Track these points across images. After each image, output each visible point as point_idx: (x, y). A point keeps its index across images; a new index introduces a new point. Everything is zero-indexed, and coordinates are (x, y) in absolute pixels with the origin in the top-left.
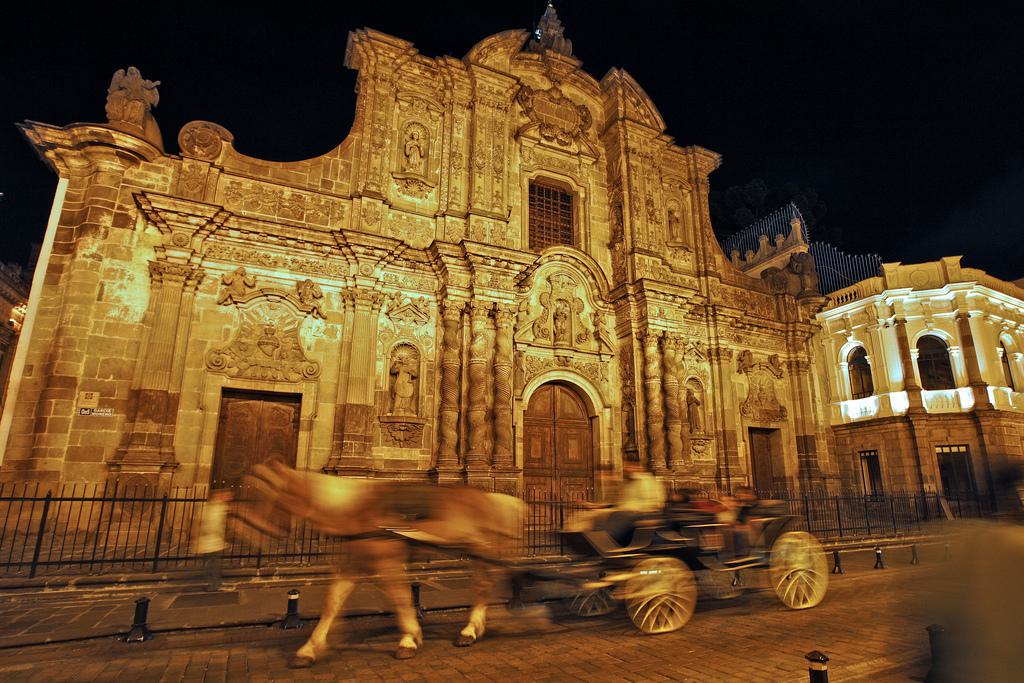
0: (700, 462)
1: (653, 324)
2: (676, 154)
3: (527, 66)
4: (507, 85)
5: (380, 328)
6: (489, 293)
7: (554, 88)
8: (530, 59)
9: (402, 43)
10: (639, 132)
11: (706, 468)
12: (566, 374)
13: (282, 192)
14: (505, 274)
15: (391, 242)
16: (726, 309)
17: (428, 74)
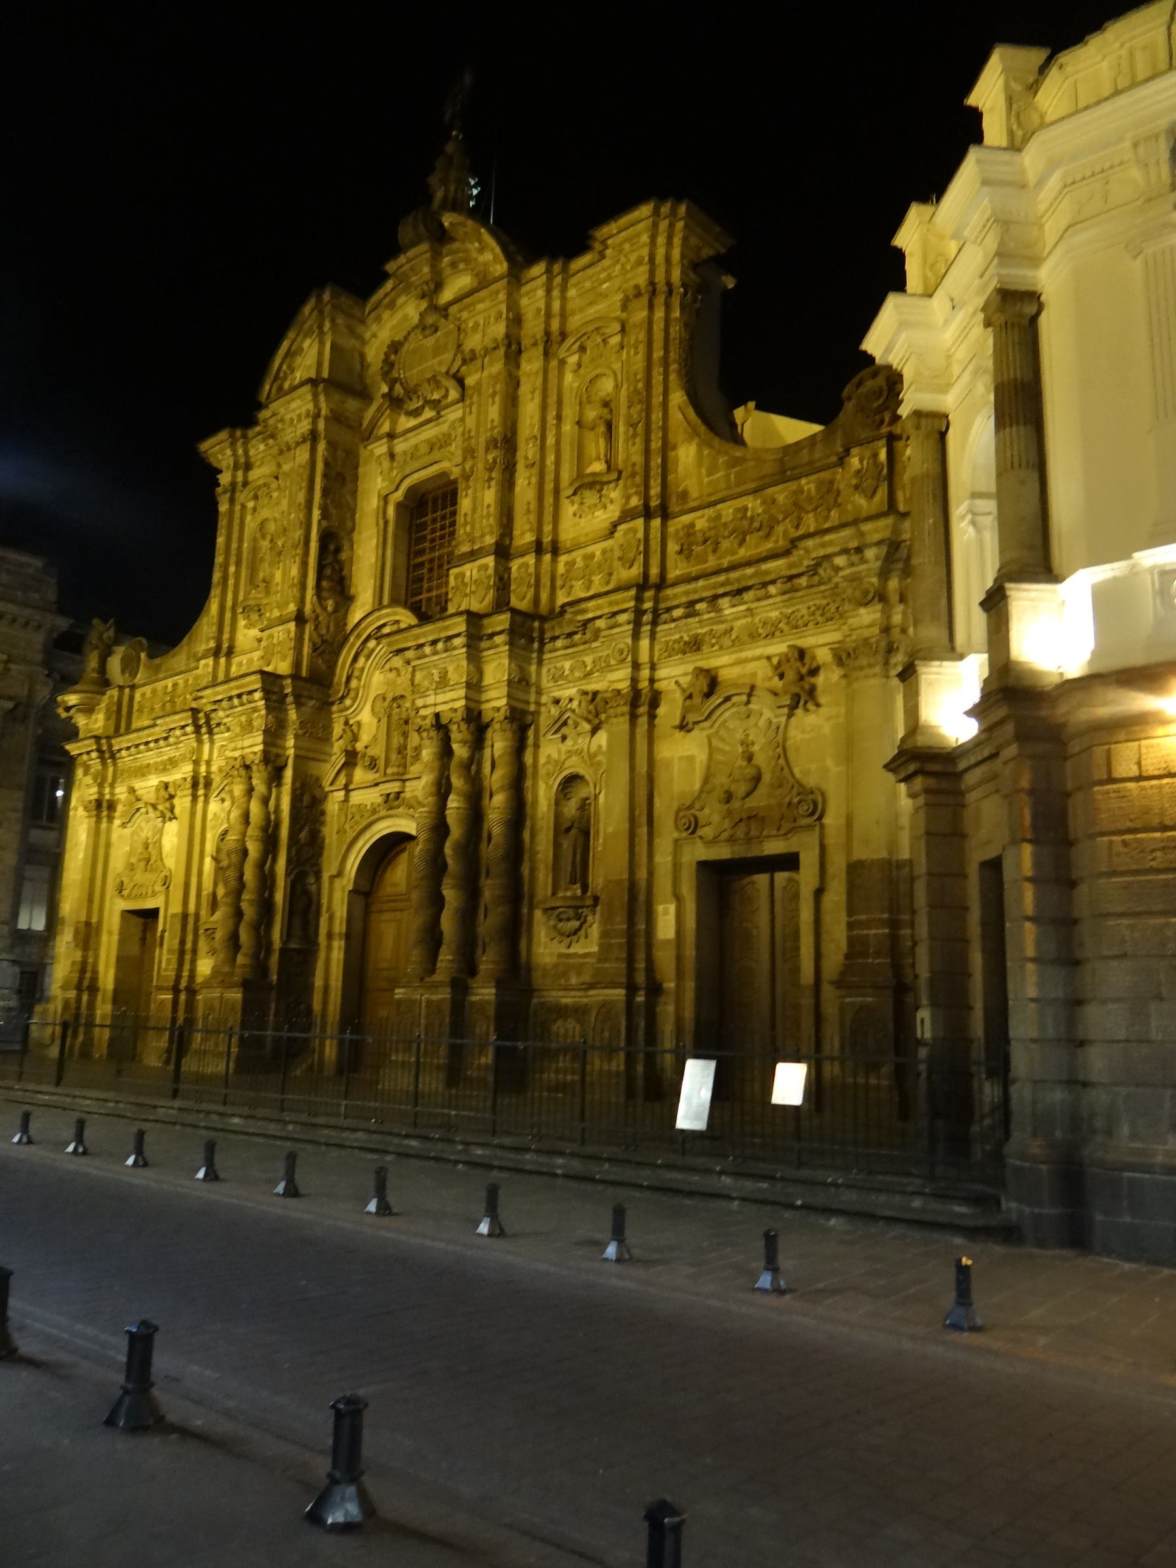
0: (569, 956)
1: (425, 707)
2: (590, 272)
3: (392, 306)
4: (309, 397)
5: (210, 816)
6: (240, 744)
7: (433, 308)
8: (387, 295)
9: (223, 435)
10: (480, 307)
11: (579, 969)
12: (397, 821)
13: (166, 687)
14: (255, 710)
15: (184, 715)
16: (591, 604)
17: (271, 441)
